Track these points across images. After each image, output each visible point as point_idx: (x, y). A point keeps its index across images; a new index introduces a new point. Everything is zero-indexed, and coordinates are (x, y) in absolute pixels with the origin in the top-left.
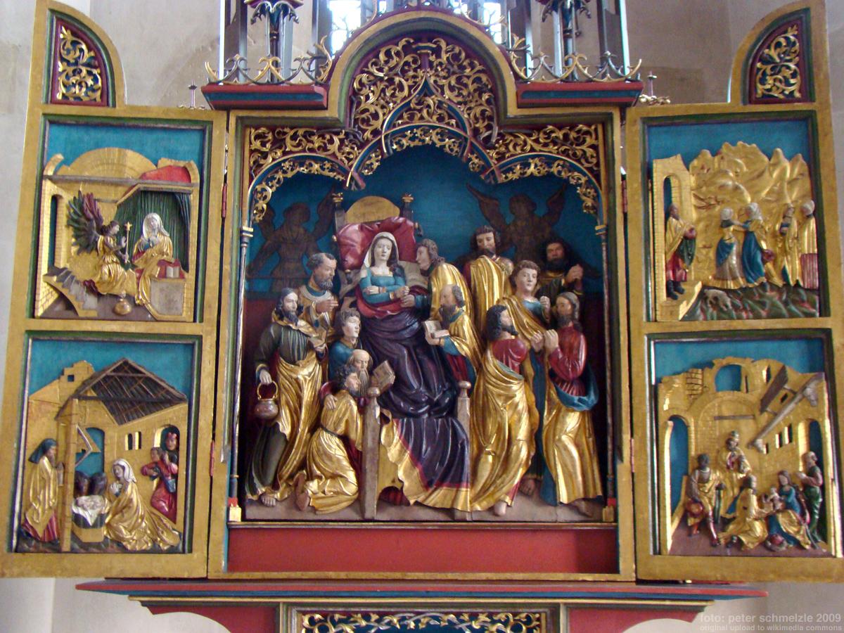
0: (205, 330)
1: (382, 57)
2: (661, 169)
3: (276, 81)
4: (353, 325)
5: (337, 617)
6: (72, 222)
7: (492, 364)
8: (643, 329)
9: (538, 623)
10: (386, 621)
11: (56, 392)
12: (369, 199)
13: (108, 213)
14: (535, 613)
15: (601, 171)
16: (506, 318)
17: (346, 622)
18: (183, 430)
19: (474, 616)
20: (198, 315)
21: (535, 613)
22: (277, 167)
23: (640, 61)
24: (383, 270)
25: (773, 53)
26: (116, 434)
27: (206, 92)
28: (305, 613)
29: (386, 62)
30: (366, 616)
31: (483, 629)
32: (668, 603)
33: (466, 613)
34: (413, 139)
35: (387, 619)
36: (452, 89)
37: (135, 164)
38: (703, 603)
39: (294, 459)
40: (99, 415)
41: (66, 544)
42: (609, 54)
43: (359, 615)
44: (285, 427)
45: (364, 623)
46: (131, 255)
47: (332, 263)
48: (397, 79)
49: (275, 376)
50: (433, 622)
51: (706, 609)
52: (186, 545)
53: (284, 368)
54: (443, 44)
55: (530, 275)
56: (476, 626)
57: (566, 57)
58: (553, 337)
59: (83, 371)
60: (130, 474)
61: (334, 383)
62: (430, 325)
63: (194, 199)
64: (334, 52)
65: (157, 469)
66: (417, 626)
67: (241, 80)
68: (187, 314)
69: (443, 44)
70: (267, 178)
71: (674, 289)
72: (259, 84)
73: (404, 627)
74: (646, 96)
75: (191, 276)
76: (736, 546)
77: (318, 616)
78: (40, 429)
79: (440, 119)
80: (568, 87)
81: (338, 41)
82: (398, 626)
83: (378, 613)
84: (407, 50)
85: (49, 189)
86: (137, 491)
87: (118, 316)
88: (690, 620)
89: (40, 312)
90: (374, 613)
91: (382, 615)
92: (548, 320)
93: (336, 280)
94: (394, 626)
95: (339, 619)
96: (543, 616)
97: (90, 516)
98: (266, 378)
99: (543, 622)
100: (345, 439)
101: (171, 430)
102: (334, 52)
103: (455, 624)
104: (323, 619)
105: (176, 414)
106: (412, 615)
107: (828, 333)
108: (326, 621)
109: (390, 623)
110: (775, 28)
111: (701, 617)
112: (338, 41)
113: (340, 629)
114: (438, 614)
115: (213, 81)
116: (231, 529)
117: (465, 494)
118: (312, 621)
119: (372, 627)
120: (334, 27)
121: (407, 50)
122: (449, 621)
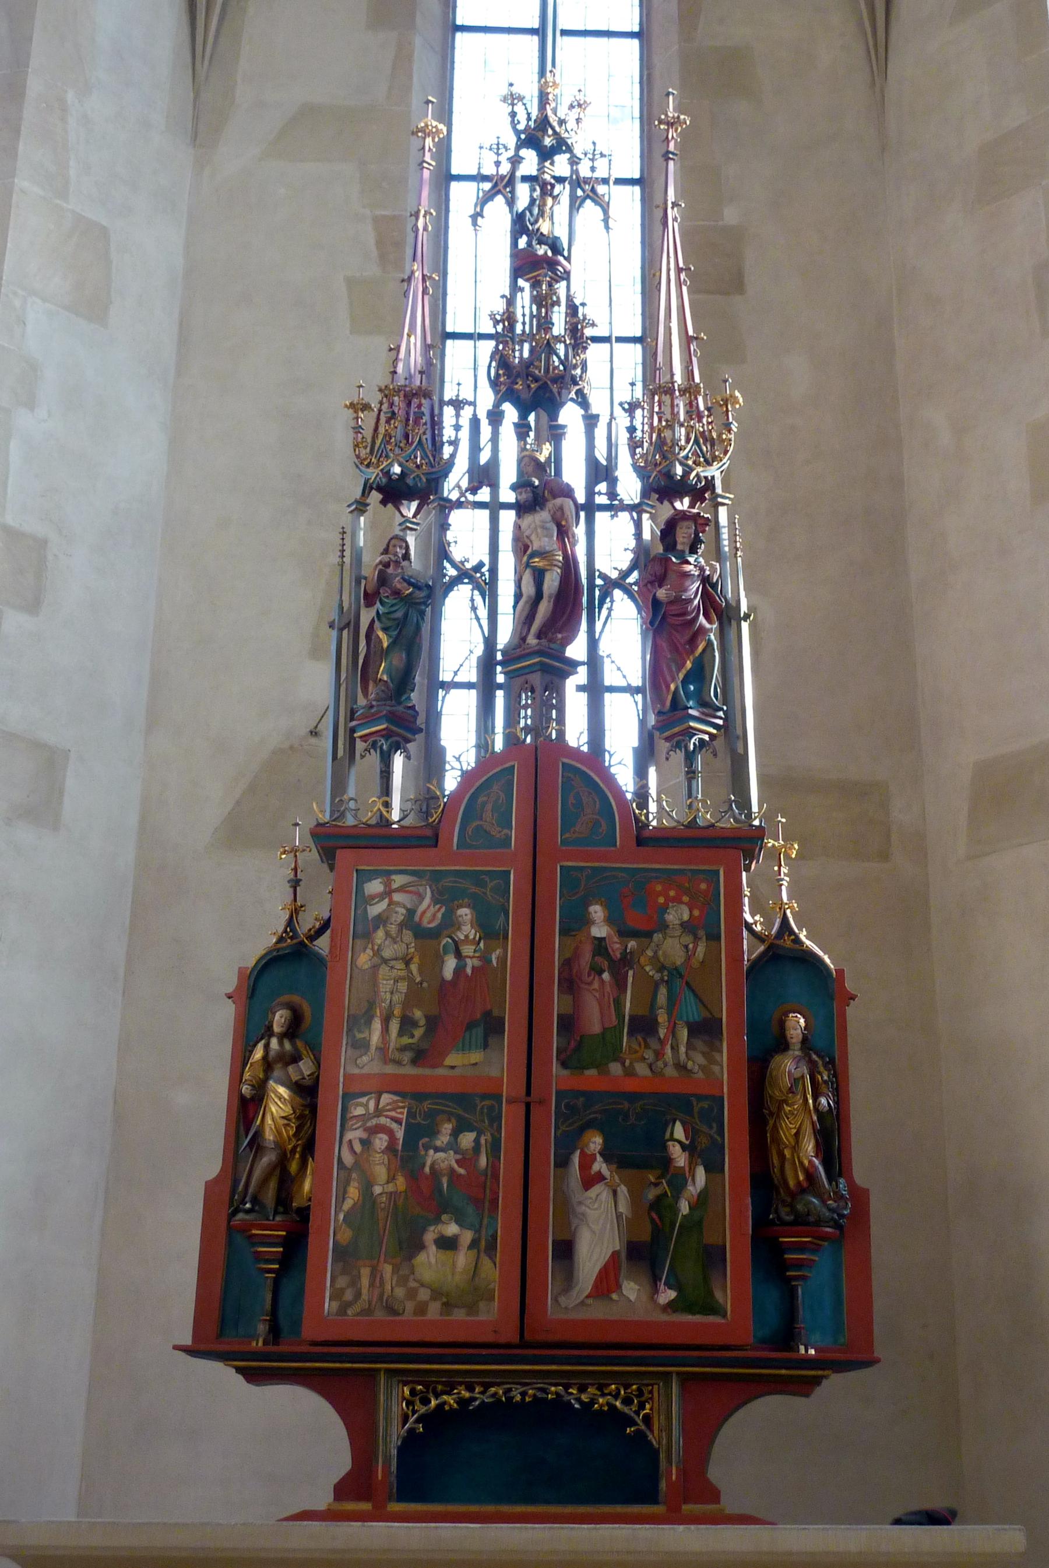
3: (384, 823)
5: (440, 1387)
9: (650, 1396)
10: (492, 1392)
14: (648, 1385)
17: (449, 1393)
19: (582, 1389)
21: (648, 1385)
23: (765, 805)
27: (314, 834)
28: (405, 1384)
30: (470, 1388)
31: (593, 1402)
32: (783, 1372)
33: (575, 1384)
35: (493, 1390)
38: (820, 1373)
42: (733, 798)
43: (463, 1387)
45: (466, 1394)
50: (539, 1395)
51: (825, 1382)
56: (584, 1397)
57: (690, 800)
64: (447, 793)
66: (523, 1399)
67: (350, 821)
72: (369, 826)
73: (510, 1399)
74: (772, 841)
77: (420, 1387)
80: (690, 833)
81: (451, 783)
82: (504, 1399)
83: (481, 1384)
88: (807, 1395)
90: (479, 1383)
91: (486, 1386)
94: (499, 1401)
95: (441, 1391)
96: (656, 1387)
99: (656, 1394)
102: (447, 793)
103: (563, 1396)
104: (425, 1390)
106: (519, 1386)
108: (428, 1392)
109: (495, 1395)
111: (819, 1391)
112: (451, 783)
113: (442, 1400)
114: (546, 1386)
115: (321, 821)
118: (413, 1392)
119: (475, 1399)
120: (447, 767)
122: (557, 1393)
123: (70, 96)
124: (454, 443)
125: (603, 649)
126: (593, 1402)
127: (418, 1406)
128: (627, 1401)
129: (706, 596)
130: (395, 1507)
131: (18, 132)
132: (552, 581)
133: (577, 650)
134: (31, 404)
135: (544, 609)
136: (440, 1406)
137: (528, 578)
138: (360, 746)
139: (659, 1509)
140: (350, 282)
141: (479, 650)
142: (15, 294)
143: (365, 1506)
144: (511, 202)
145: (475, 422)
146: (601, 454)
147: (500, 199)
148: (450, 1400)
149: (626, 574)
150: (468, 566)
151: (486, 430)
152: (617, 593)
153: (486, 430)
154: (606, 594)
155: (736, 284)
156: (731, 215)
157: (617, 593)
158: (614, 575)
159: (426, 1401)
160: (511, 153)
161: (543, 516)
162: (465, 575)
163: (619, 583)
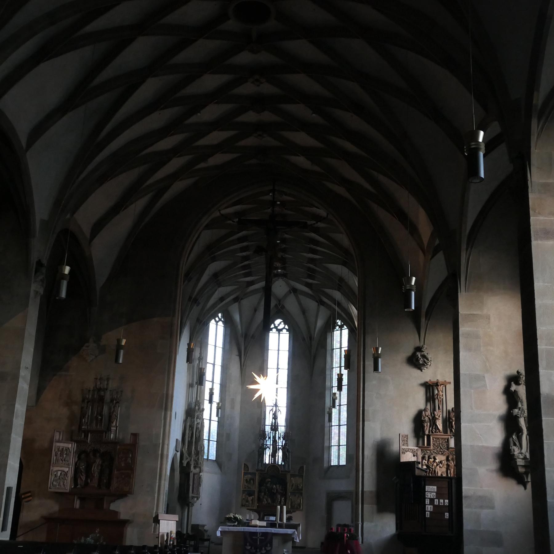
2: (291, 479)
4: (267, 490)
11: (244, 495)
13: (248, 480)
16: (279, 490)
24: (269, 485)
37: (250, 476)
40: (247, 496)
44: (261, 498)
55: (281, 486)
59: (246, 493)
61: (265, 494)
65: (252, 500)
71: (292, 488)
78: (244, 497)
85: (244, 478)
86: (251, 502)
97: (247, 504)
101: (253, 498)
105: (253, 497)
116: (257, 506)
117: (275, 504)
125: (279, 455)
129: (287, 451)
131: (226, 391)
132: (275, 449)
144: (273, 411)
145: (269, 433)
147: (271, 411)
151: (270, 433)
153: (270, 433)
162: (268, 447)
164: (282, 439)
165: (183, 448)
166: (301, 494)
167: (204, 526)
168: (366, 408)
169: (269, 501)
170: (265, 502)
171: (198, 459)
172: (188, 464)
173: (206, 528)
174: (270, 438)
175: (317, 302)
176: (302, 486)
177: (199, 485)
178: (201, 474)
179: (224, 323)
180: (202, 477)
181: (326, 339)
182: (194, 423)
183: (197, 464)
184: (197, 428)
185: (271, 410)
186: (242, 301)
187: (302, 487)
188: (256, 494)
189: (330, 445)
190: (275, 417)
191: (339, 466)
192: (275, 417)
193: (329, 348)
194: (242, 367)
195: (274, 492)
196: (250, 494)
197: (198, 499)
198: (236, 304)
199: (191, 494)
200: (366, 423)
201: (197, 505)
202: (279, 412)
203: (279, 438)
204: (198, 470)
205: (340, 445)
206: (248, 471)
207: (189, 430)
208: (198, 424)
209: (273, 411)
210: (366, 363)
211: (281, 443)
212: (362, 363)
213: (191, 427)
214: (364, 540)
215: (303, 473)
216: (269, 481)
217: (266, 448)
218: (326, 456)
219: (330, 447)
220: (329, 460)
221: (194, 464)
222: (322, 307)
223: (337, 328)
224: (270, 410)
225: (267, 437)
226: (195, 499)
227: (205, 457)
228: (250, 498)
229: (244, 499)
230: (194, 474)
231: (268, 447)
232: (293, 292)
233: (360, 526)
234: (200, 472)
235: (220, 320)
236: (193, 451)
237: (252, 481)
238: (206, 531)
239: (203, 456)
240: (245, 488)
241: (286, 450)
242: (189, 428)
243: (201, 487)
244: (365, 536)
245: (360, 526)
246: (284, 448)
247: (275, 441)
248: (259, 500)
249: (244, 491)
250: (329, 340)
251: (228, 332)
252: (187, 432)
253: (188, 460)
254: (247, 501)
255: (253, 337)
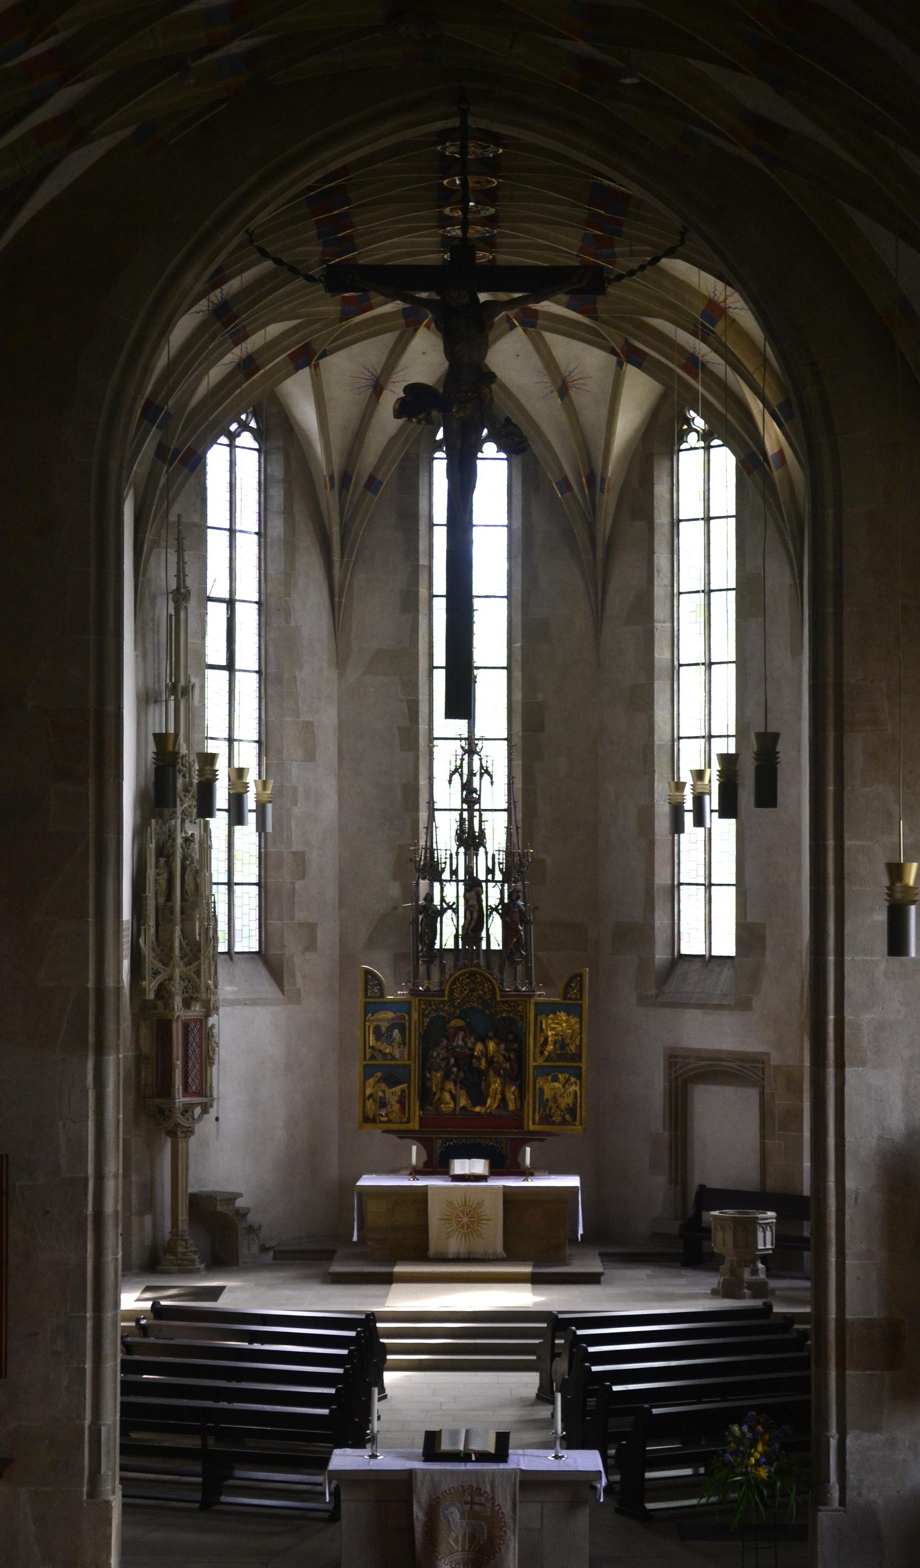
0: (411, 1063)
1: (461, 979)
4: (452, 1061)
6: (374, 1033)
7: (491, 1073)
8: (532, 1064)
11: (371, 1081)
12: (458, 1020)
13: (384, 1030)
15: (524, 1017)
18: (406, 1091)
19: (486, 1140)
20: (409, 1059)
22: (430, 1013)
24: (460, 1043)
25: (573, 985)
26: (389, 1091)
29: (462, 981)
30: (457, 1140)
34: (470, 1004)
36: (481, 990)
39: (437, 1097)
40: (383, 1086)
41: (378, 1121)
45: (456, 1142)
46: (390, 1040)
47: (445, 1042)
48: (465, 987)
49: (431, 1075)
52: (408, 1122)
53: (434, 1073)
54: (478, 976)
55: (503, 1046)
58: (508, 1065)
59: (379, 1075)
60: (393, 1103)
61: (447, 1077)
62: (474, 1061)
63: (407, 1024)
65: (401, 1102)
68: (406, 1057)
69: (478, 976)
70: (427, 1016)
75: (407, 1047)
76: (554, 1123)
78: (368, 1091)
79: (478, 999)
84: (468, 978)
85: (367, 1023)
86: (396, 1107)
87: (387, 1060)
89: (367, 1059)
92: (507, 1059)
93: (447, 1047)
97: (383, 1114)
98: (428, 1075)
100: (451, 1092)
101: (403, 1091)
107: (580, 1068)
110: (573, 978)
121: (468, 978)
123: (297, 674)
124: (445, 863)
126: (489, 1143)
127: (444, 1145)
128: (497, 1143)
130: (439, 1170)
132: (475, 915)
133: (484, 934)
134: (296, 804)
135: (473, 923)
136: (449, 1145)
137: (468, 913)
138: (420, 962)
139: (505, 1170)
140: (399, 728)
141: (454, 932)
142: (288, 764)
143: (431, 1170)
144: (461, 775)
145: (451, 855)
146: (490, 867)
147: (457, 774)
148: (452, 1143)
149: (497, 907)
150: (450, 904)
151: (454, 856)
152: (494, 913)
153: (454, 856)
154: (491, 913)
155: (541, 727)
156: (540, 697)
157: (494, 913)
158: (494, 907)
159: (446, 1144)
160: (460, 757)
161: (473, 893)
162: (450, 907)
163: (496, 909)
164: (499, 876)
165: (139, 936)
166: (577, 1072)
167: (234, 1197)
168: (848, 1017)
169: (463, 1102)
170: (448, 1106)
171: (198, 973)
172: (163, 992)
173: (240, 1203)
174: (454, 872)
175: (613, 352)
176: (578, 1042)
177: (207, 1059)
178: (212, 1020)
179: (257, 435)
180: (215, 1031)
181: (648, 483)
182: (174, 840)
183: (196, 989)
184: (184, 858)
185: (456, 771)
186: (324, 362)
187: (580, 1047)
188: (414, 1077)
189: (676, 883)
190: (470, 797)
191: (709, 961)
192: (470, 797)
193: (661, 519)
194: (336, 599)
195: (478, 1070)
196: (391, 1079)
197: (205, 1109)
198: (305, 374)
199: (180, 1100)
200: (848, 1070)
201: (205, 1127)
202: (486, 776)
203: (490, 871)
204: (197, 1009)
205: (711, 885)
206: (382, 995)
207: (157, 866)
208: (188, 840)
209: (461, 775)
210: (848, 843)
211: (493, 895)
212: (831, 843)
213: (164, 852)
214: (851, 1494)
215: (581, 998)
216: (457, 1029)
217: (442, 912)
218: (660, 921)
219: (673, 890)
220: (674, 937)
221: (185, 990)
222: (631, 371)
223: (692, 438)
224: (453, 769)
225: (443, 870)
226: (198, 1111)
227: (222, 947)
228: (392, 1094)
229: (371, 1096)
230: (186, 1026)
231: (450, 907)
232: (521, 325)
233: (833, 1443)
234: (208, 1015)
235: (244, 427)
236: (177, 944)
237: (396, 1033)
238: (242, 1214)
239: (215, 947)
240: (373, 1057)
241: (517, 916)
242: (157, 862)
243: (215, 1068)
244: (852, 1479)
245: (833, 1443)
246: (507, 911)
247: (473, 886)
248: (425, 1095)
249: (368, 1072)
250: (660, 489)
251: (277, 471)
252: (151, 873)
253: (160, 978)
254: (383, 1104)
255: (372, 484)
